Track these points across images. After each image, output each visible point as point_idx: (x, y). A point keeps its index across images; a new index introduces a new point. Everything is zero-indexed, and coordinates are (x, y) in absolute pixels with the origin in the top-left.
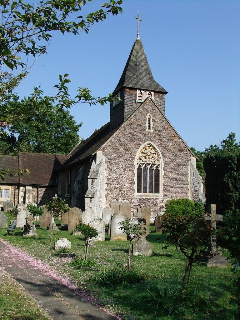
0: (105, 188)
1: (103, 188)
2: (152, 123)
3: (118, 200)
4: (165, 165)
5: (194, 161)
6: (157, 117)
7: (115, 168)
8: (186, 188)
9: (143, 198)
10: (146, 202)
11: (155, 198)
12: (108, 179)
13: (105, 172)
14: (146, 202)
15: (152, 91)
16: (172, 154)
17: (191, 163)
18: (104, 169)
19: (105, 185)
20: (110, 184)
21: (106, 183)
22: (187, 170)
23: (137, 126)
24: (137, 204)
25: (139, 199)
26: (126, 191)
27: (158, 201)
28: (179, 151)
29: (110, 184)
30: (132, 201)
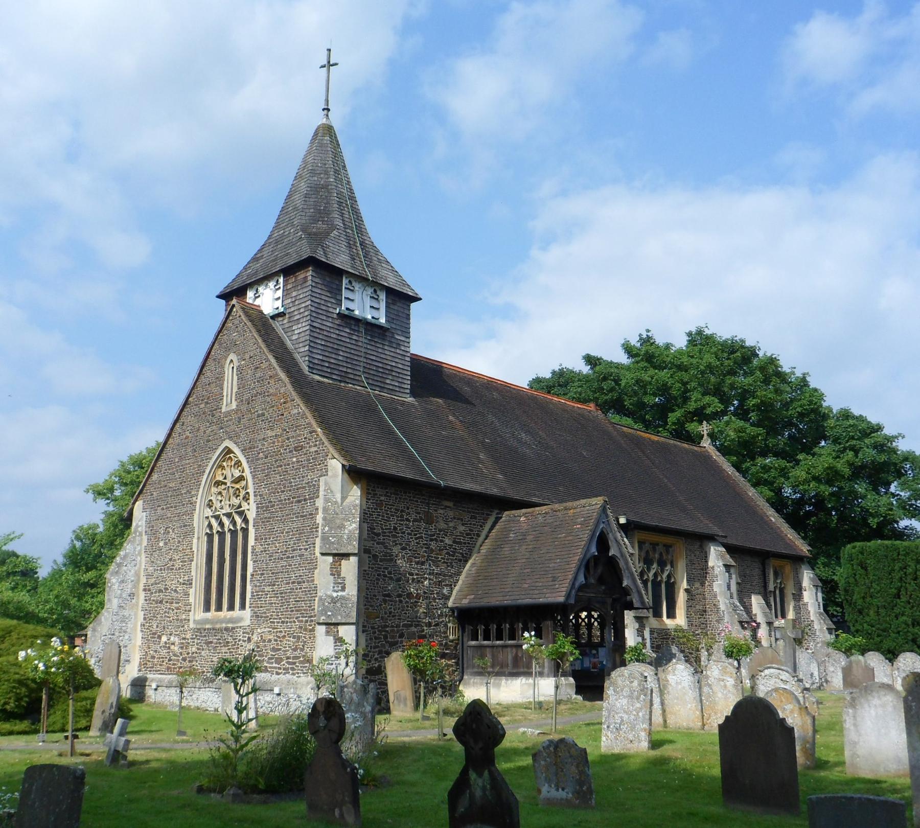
0: (140, 605)
1: (137, 605)
2: (235, 378)
3: (160, 637)
4: (258, 508)
5: (335, 476)
6: (247, 356)
7: (161, 544)
8: (308, 581)
9: (207, 626)
10: (211, 642)
11: (230, 625)
12: (149, 576)
13: (143, 555)
14: (211, 642)
15: (277, 274)
16: (278, 467)
17: (326, 484)
18: (140, 550)
19: (142, 595)
20: (149, 590)
21: (145, 590)
22: (312, 516)
23: (207, 403)
24: (194, 649)
25: (199, 631)
26: (178, 609)
27: (240, 634)
28: (296, 449)
29: (149, 590)
30: (184, 639)
